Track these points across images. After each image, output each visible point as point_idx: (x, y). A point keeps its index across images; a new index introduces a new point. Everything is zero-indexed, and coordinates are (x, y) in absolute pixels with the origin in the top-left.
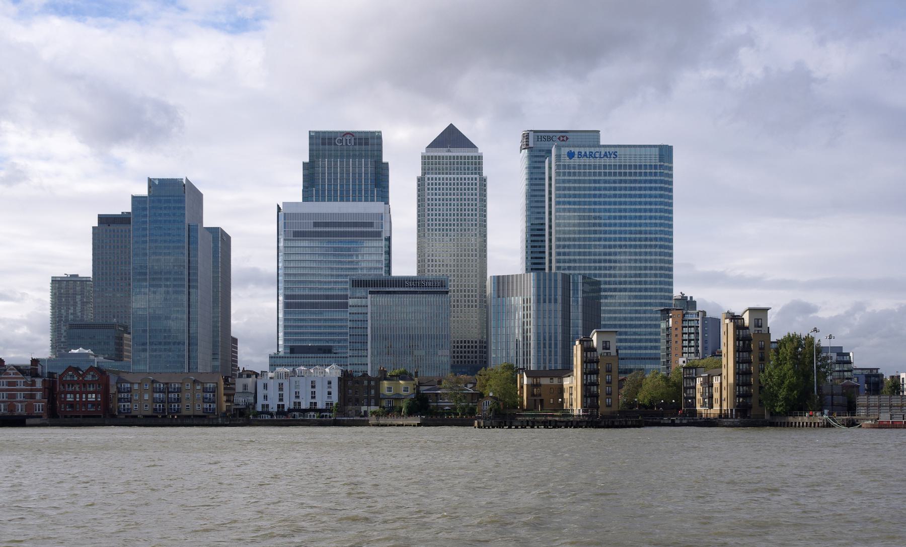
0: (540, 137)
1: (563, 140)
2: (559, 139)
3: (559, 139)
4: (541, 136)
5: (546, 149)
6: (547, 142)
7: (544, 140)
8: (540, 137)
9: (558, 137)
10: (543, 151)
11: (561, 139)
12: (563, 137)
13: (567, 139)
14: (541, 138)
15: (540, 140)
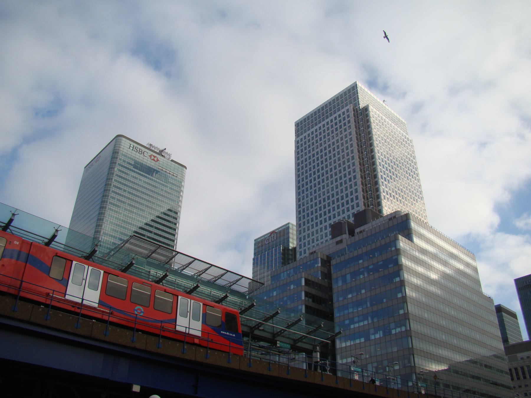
0: (132, 146)
1: (154, 160)
2: (150, 156)
3: (150, 156)
4: (134, 146)
5: (136, 159)
6: (137, 154)
7: (136, 151)
8: (132, 146)
9: (150, 155)
10: (132, 159)
11: (153, 158)
12: (155, 157)
13: (158, 160)
14: (133, 148)
15: (131, 148)
